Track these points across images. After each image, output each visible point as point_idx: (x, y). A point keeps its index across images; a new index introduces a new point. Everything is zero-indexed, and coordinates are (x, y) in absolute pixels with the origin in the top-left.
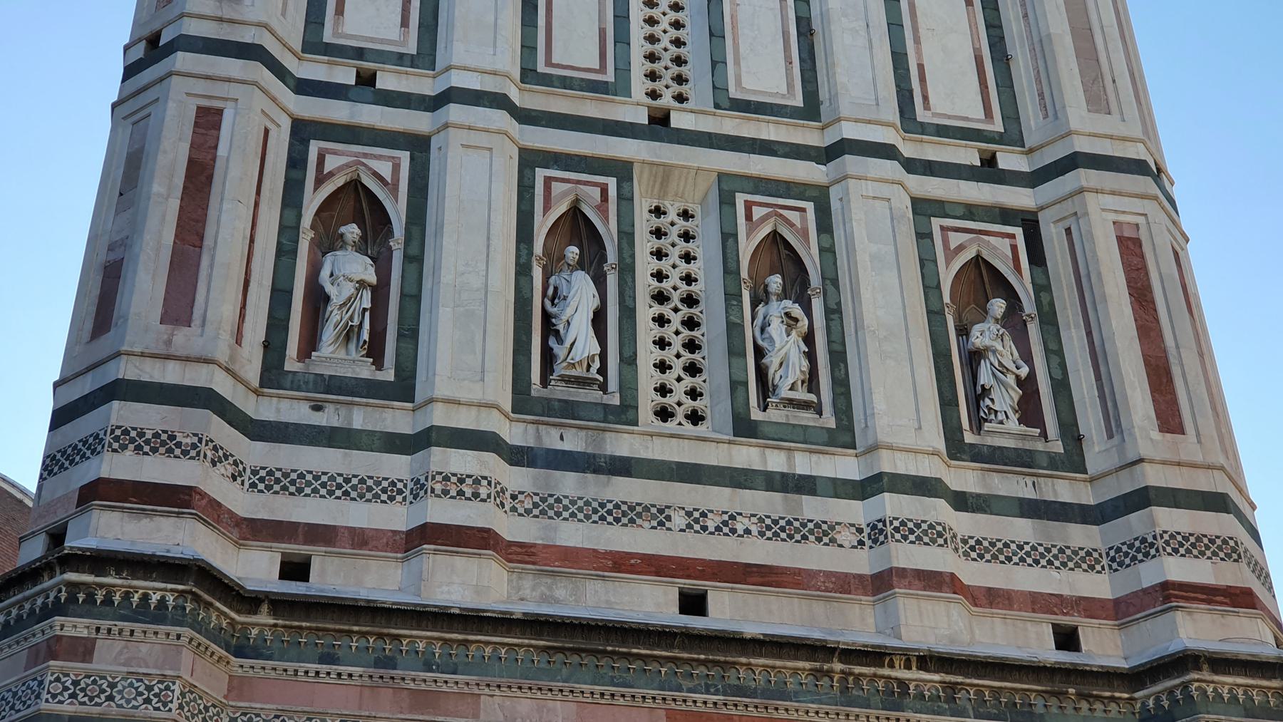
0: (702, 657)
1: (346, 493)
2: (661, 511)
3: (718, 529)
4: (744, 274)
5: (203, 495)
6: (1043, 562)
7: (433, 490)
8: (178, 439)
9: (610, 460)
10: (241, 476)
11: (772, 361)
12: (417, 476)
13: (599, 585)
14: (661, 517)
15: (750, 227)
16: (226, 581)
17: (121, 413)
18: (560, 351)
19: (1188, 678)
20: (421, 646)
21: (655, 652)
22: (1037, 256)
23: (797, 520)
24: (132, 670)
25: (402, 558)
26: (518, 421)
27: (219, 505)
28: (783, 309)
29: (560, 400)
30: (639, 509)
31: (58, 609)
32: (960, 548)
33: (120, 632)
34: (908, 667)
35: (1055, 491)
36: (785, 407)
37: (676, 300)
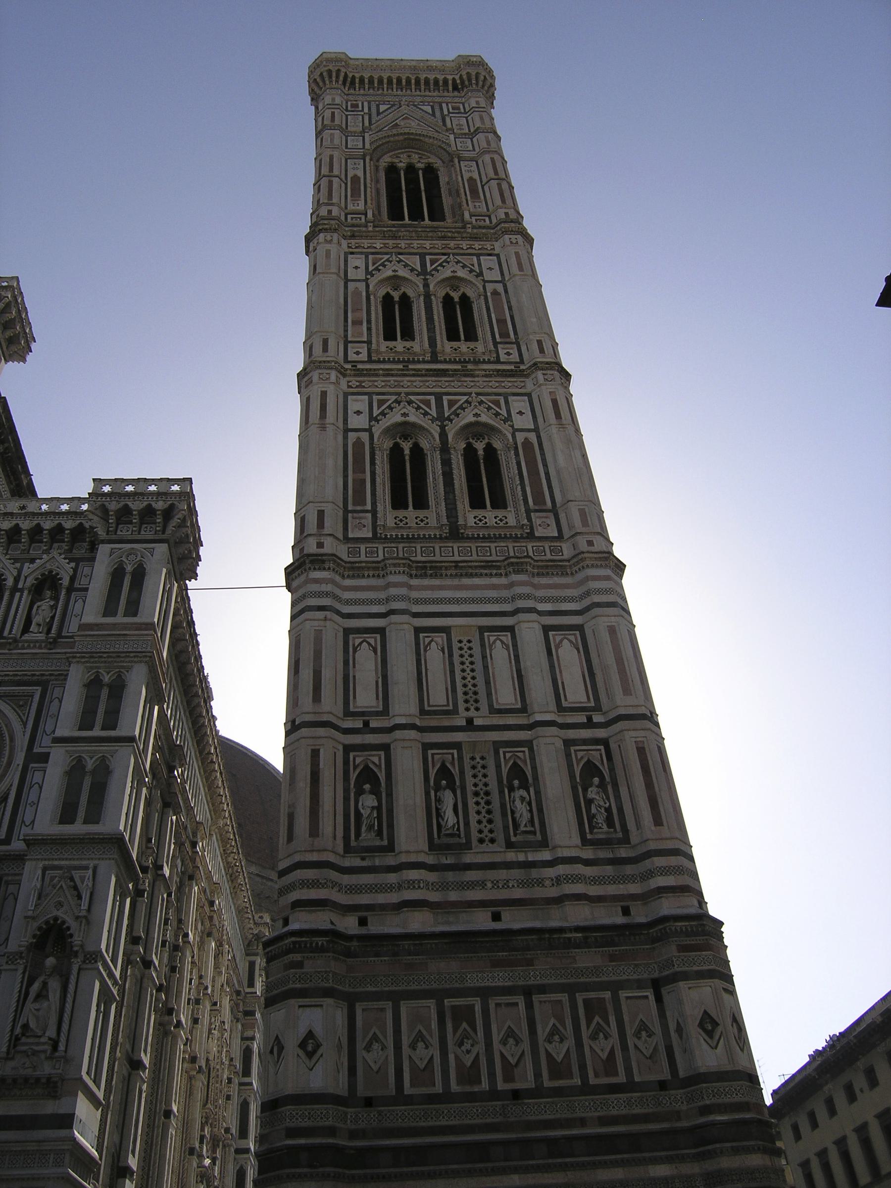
1: (376, 891)
2: (483, 883)
3: (503, 886)
4: (505, 782)
5: (331, 901)
11: (517, 815)
14: (482, 884)
18: (443, 823)
37: (482, 795)
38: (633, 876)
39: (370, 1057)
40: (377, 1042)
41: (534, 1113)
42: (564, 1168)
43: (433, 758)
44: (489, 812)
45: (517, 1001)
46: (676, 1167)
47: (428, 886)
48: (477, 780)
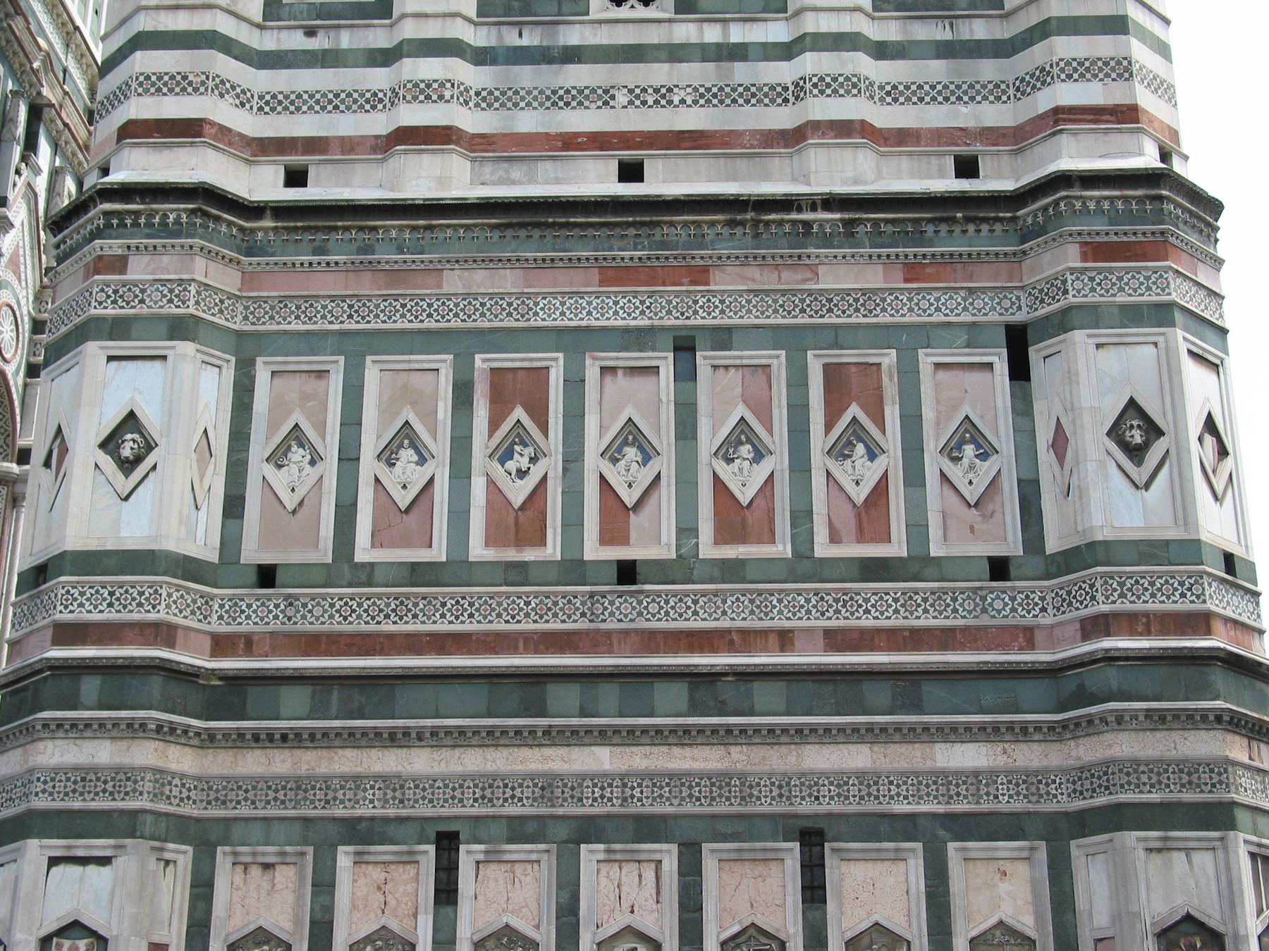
0: (631, 219)
1: (336, 107)
2: (606, 92)
5: (212, 124)
6: (953, 99)
8: (190, 79)
10: (249, 101)
13: (549, 165)
14: (605, 97)
17: (145, 61)
19: (1058, 195)
21: (590, 220)
24: (157, 277)
27: (229, 130)
30: (587, 92)
31: (97, 234)
33: (146, 248)
35: (971, 31)
38: (996, 86)
39: (280, 480)
40: (301, 445)
41: (667, 613)
42: (725, 736)
45: (654, 363)
46: (1005, 753)
47: (465, 97)
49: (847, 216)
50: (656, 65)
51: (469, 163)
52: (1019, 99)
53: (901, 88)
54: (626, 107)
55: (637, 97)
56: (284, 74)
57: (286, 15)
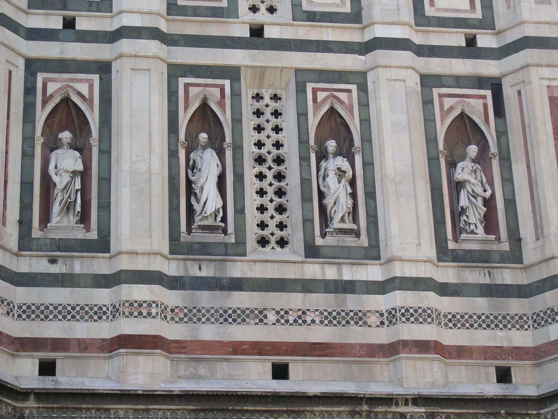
0: (285, 409)
1: (73, 317)
2: (261, 312)
3: (295, 321)
4: (312, 142)
6: (493, 326)
7: (124, 313)
9: (230, 280)
11: (329, 201)
12: (114, 303)
13: (224, 365)
15: (316, 107)
16: (9, 386)
18: (197, 207)
20: (121, 414)
21: (257, 408)
22: (499, 111)
23: (343, 311)
25: (108, 357)
26: (173, 259)
28: (336, 165)
29: (198, 243)
30: (247, 312)
32: (443, 321)
34: (406, 404)
35: (503, 278)
36: (337, 234)
37: (270, 162)
38: (521, 318)
43: (186, 92)
44: (280, 193)
48: (262, 137)
49: (429, 411)
50: (294, 294)
51: (169, 361)
52: (536, 328)
53: (458, 317)
54: (274, 324)
55: (282, 317)
56: (36, 290)
57: (35, 247)
